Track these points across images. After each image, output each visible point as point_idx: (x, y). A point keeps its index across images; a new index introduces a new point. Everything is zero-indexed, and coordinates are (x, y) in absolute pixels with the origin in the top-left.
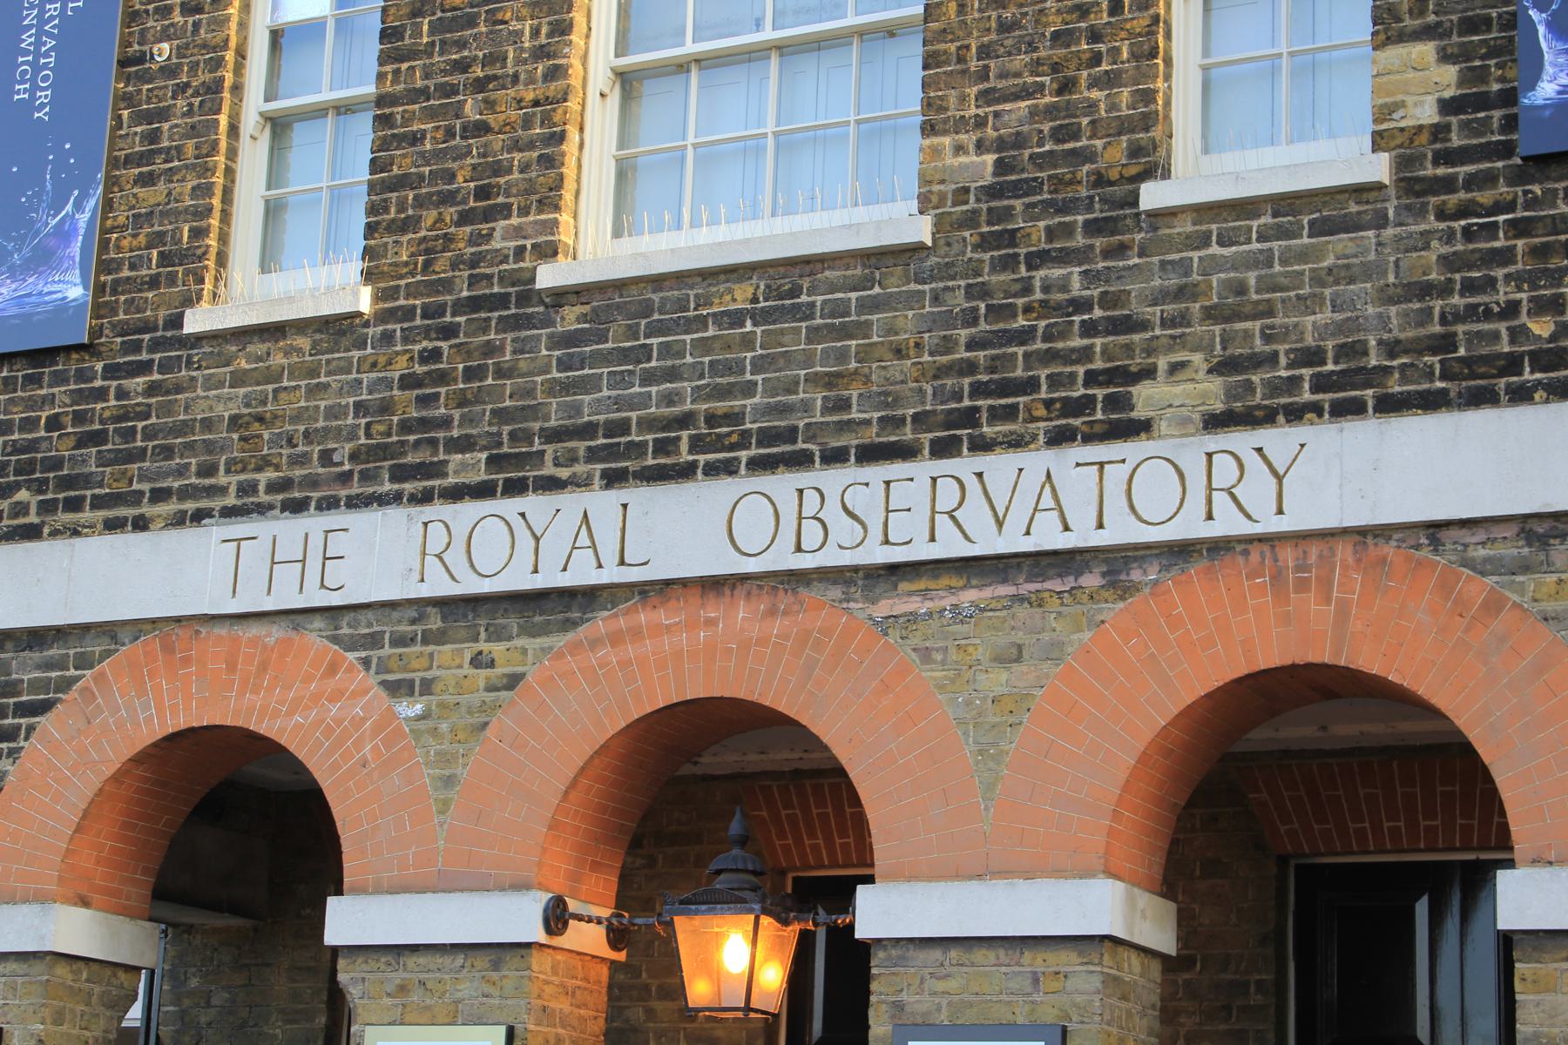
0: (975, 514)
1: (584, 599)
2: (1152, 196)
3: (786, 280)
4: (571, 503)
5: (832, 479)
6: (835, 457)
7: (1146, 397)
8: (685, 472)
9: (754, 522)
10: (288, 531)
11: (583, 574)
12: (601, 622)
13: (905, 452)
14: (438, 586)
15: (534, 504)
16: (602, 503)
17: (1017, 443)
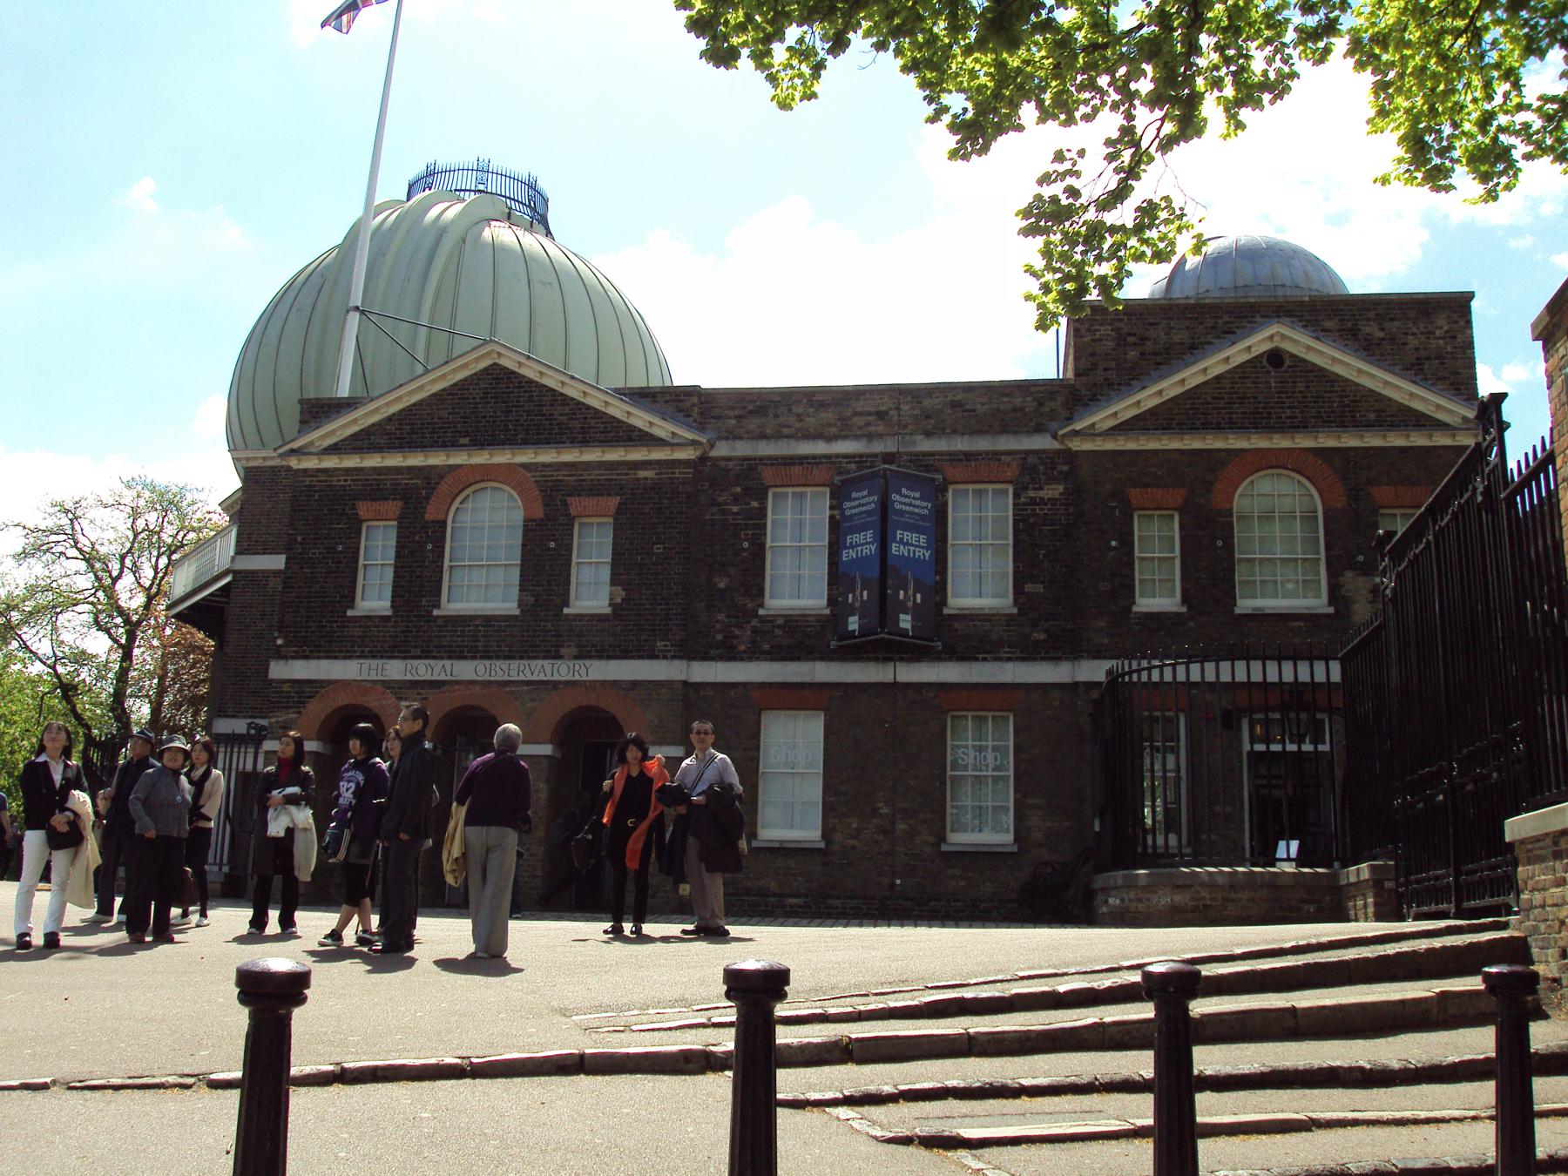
0: (527, 672)
1: (443, 683)
2: (566, 611)
3: (488, 620)
4: (440, 663)
5: (498, 663)
6: (498, 658)
7: (563, 651)
8: (465, 658)
9: (481, 669)
10: (374, 663)
11: (443, 677)
12: (446, 688)
13: (513, 658)
14: (409, 677)
15: (432, 662)
16: (448, 663)
17: (536, 658)
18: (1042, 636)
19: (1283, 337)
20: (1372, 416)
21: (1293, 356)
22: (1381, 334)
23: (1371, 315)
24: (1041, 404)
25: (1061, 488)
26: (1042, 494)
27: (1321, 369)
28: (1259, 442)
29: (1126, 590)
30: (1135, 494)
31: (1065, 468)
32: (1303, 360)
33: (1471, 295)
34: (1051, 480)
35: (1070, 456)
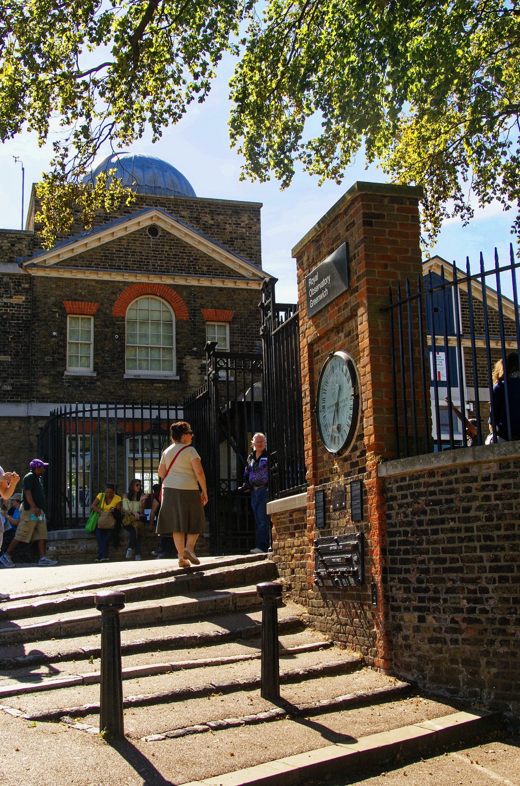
18: (9, 388)
19: (158, 218)
20: (205, 269)
21: (163, 230)
22: (212, 222)
23: (207, 210)
24: (13, 245)
25: (24, 298)
26: (11, 301)
27: (178, 239)
28: (143, 279)
29: (60, 360)
30: (68, 305)
31: (27, 286)
32: (169, 233)
33: (261, 205)
34: (17, 293)
35: (31, 279)
